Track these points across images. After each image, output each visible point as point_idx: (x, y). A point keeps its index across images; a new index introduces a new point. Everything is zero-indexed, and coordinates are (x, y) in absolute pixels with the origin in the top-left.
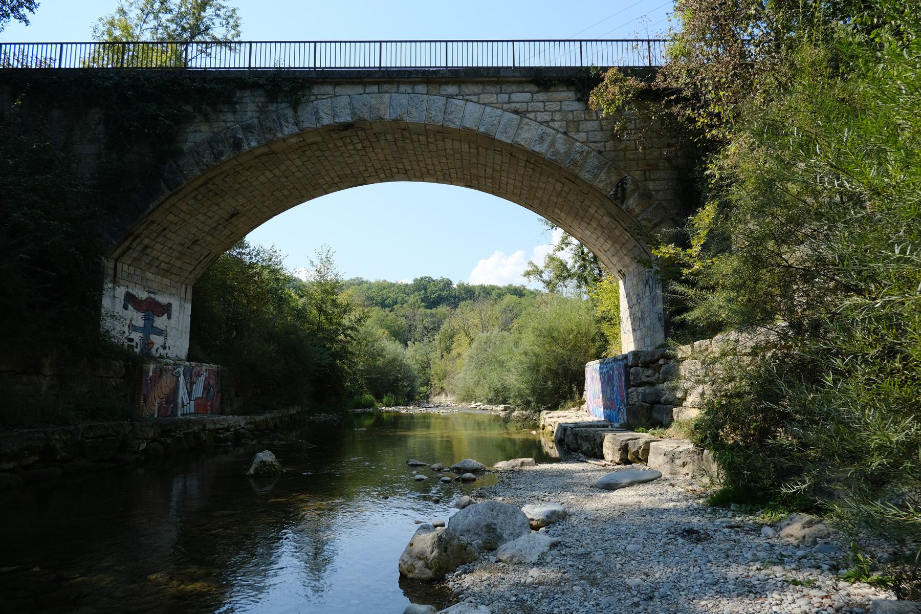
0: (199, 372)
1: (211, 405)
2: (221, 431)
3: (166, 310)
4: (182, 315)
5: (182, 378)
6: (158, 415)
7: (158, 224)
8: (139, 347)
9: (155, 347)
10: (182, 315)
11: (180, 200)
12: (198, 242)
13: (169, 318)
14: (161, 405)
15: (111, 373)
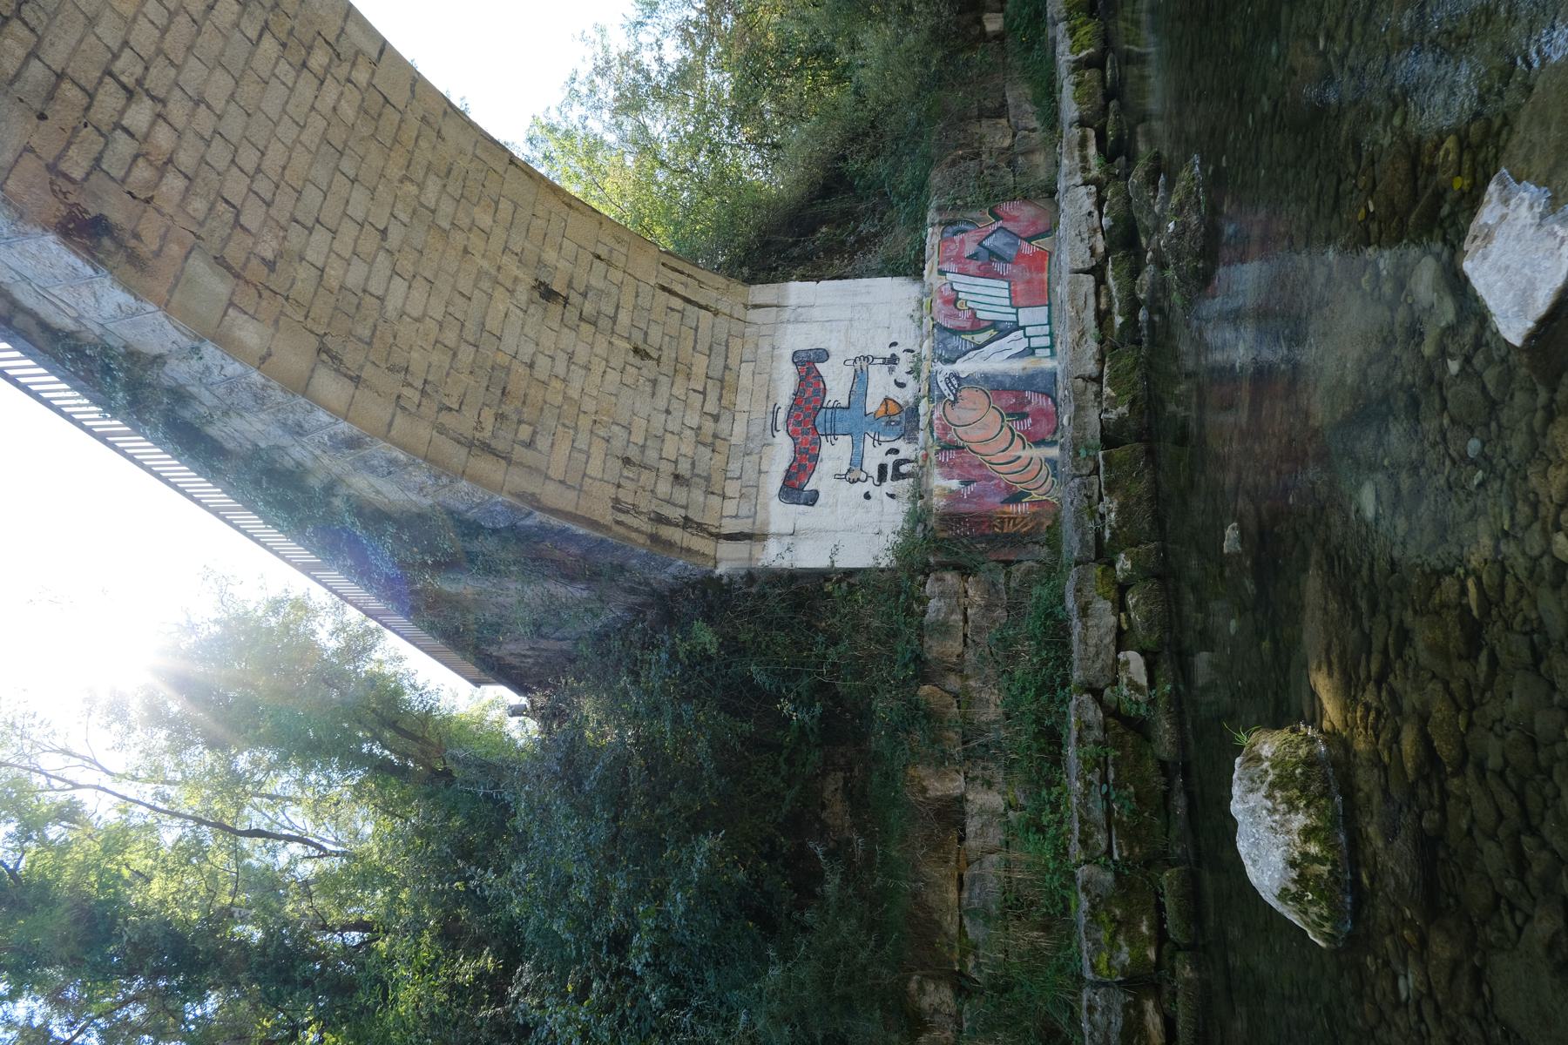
0: (947, 302)
1: (1029, 240)
2: (1103, 300)
3: (808, 363)
5: (963, 367)
7: (619, 486)
8: (895, 445)
9: (895, 393)
11: (547, 477)
12: (641, 346)
13: (823, 355)
15: (957, 617)
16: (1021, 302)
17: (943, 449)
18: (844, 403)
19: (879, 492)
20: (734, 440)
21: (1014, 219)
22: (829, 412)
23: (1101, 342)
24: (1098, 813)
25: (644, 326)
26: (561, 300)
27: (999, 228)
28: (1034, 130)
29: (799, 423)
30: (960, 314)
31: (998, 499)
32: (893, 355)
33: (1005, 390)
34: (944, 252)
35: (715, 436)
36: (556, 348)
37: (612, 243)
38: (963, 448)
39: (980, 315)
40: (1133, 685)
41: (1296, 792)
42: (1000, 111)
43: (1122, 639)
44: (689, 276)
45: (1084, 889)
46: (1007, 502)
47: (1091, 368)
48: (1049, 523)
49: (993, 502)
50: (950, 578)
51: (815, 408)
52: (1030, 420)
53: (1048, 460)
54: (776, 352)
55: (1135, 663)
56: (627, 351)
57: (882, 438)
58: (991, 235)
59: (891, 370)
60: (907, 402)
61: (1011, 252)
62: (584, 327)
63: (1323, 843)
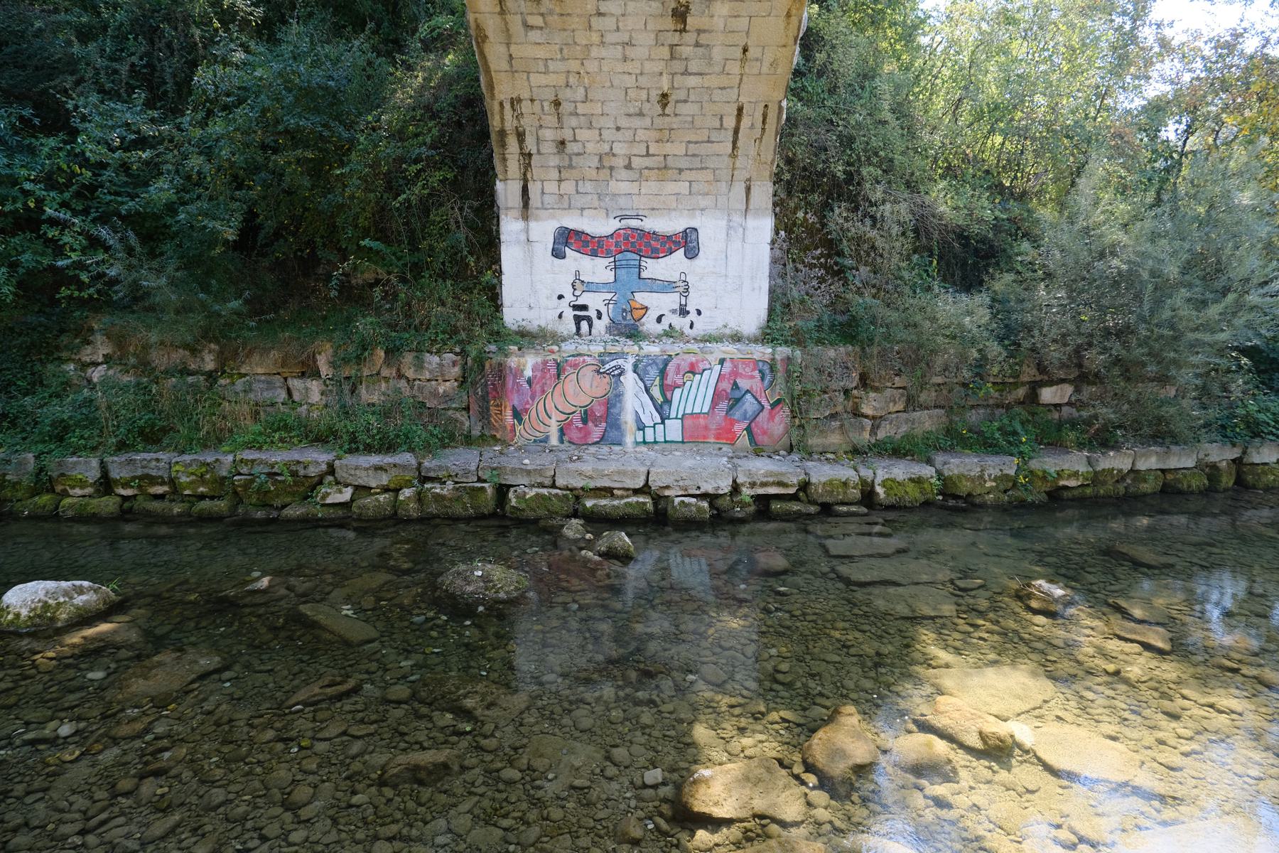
1: (749, 430)
3: (687, 243)
5: (630, 380)
6: (562, 442)
7: (532, 100)
8: (605, 316)
11: (508, 45)
12: (672, 99)
13: (692, 254)
14: (571, 423)
16: (688, 422)
17: (558, 365)
18: (644, 275)
19: (564, 306)
20: (612, 183)
21: (772, 417)
23: (582, 489)
24: (257, 470)
25: (692, 98)
26: (680, 26)
27: (763, 407)
28: (874, 431)
29: (626, 238)
31: (516, 403)
32: (688, 313)
35: (611, 168)
36: (630, 31)
37: (768, 57)
39: (677, 392)
40: (328, 494)
41: (39, 612)
42: (912, 403)
43: (361, 490)
44: (763, 129)
45: (217, 460)
46: (514, 409)
47: (560, 482)
48: (498, 436)
50: (456, 371)
54: (698, 212)
55: (347, 495)
56: (660, 88)
59: (674, 311)
61: (737, 414)
62: (665, 52)
63: (12, 622)
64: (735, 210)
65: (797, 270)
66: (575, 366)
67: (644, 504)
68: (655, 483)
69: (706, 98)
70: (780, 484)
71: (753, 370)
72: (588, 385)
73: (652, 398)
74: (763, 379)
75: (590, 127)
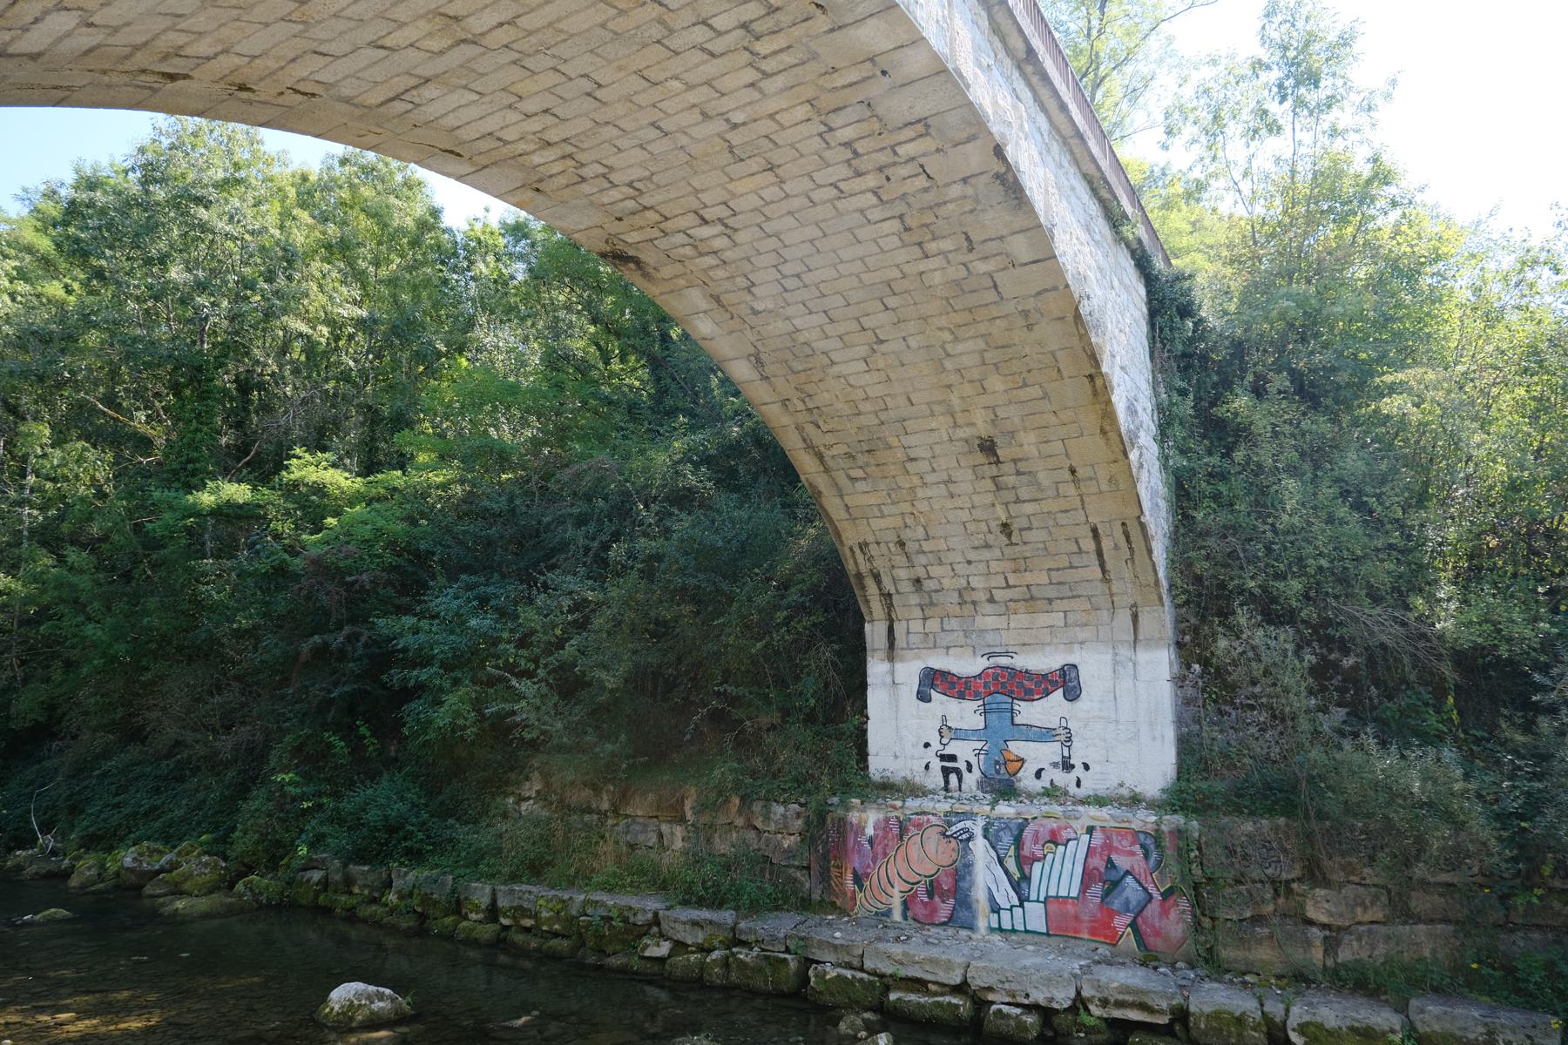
3: (1066, 682)
4: (1126, 684)
5: (979, 846)
6: (905, 918)
7: (878, 543)
8: (975, 769)
10: (1126, 684)
12: (1015, 526)
13: (1073, 694)
18: (1018, 720)
19: (930, 756)
20: (979, 619)
21: (1165, 912)
22: (1009, 706)
27: (1151, 897)
29: (995, 678)
30: (1039, 846)
31: (856, 865)
32: (1073, 767)
33: (956, 881)
34: (1118, 834)
35: (974, 603)
38: (901, 839)
39: (1037, 866)
40: (647, 946)
43: (679, 946)
46: (855, 872)
48: (838, 903)
49: (856, 862)
51: (1012, 692)
52: (926, 900)
53: (890, 910)
54: (1076, 646)
55: (663, 949)
57: (982, 757)
58: (1141, 885)
59: (1055, 765)
60: (1020, 781)
61: (1117, 904)
62: (989, 485)
64: (1122, 642)
65: (1221, 713)
66: (919, 826)
67: (957, 1006)
68: (977, 982)
69: (1051, 523)
70: (1143, 1007)
71: (1132, 844)
72: (933, 851)
73: (1006, 872)
74: (1146, 856)
75: (941, 563)
